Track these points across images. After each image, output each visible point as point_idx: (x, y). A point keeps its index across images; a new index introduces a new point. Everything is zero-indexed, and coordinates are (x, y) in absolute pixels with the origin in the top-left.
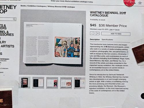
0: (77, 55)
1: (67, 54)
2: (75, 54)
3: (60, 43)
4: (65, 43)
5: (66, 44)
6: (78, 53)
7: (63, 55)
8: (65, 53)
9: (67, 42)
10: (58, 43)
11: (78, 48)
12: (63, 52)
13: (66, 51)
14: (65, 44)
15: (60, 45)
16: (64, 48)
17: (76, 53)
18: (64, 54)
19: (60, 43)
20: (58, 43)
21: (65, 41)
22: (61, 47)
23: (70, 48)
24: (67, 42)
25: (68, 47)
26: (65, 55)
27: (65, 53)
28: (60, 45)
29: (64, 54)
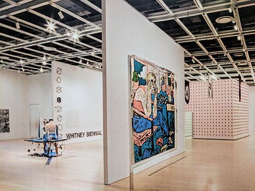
0: (170, 110)
1: (158, 107)
2: (169, 107)
3: (143, 75)
4: (152, 78)
5: (155, 82)
6: (172, 105)
7: (150, 109)
8: (153, 104)
9: (155, 77)
10: (139, 75)
11: (172, 95)
12: (150, 102)
13: (155, 98)
14: (152, 80)
15: (143, 82)
16: (150, 91)
17: (170, 105)
18: (152, 108)
19: (143, 75)
20: (139, 75)
21: (153, 75)
22: (146, 86)
23: (162, 93)
24: (155, 77)
25: (159, 92)
26: (154, 109)
27: (153, 104)
28: (143, 82)
29: (152, 108)
